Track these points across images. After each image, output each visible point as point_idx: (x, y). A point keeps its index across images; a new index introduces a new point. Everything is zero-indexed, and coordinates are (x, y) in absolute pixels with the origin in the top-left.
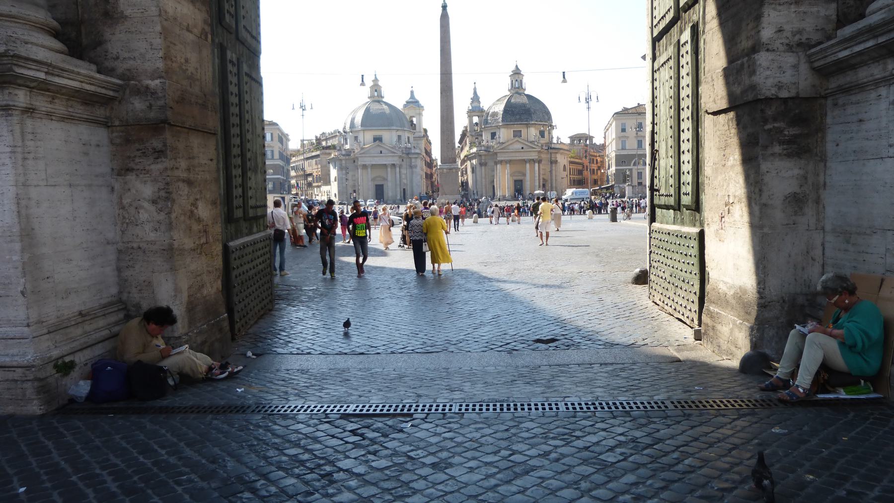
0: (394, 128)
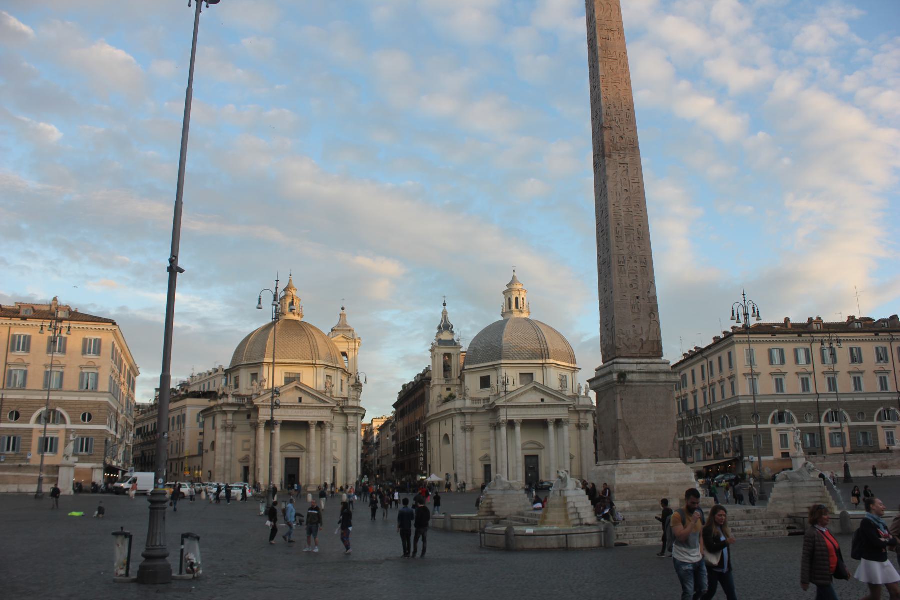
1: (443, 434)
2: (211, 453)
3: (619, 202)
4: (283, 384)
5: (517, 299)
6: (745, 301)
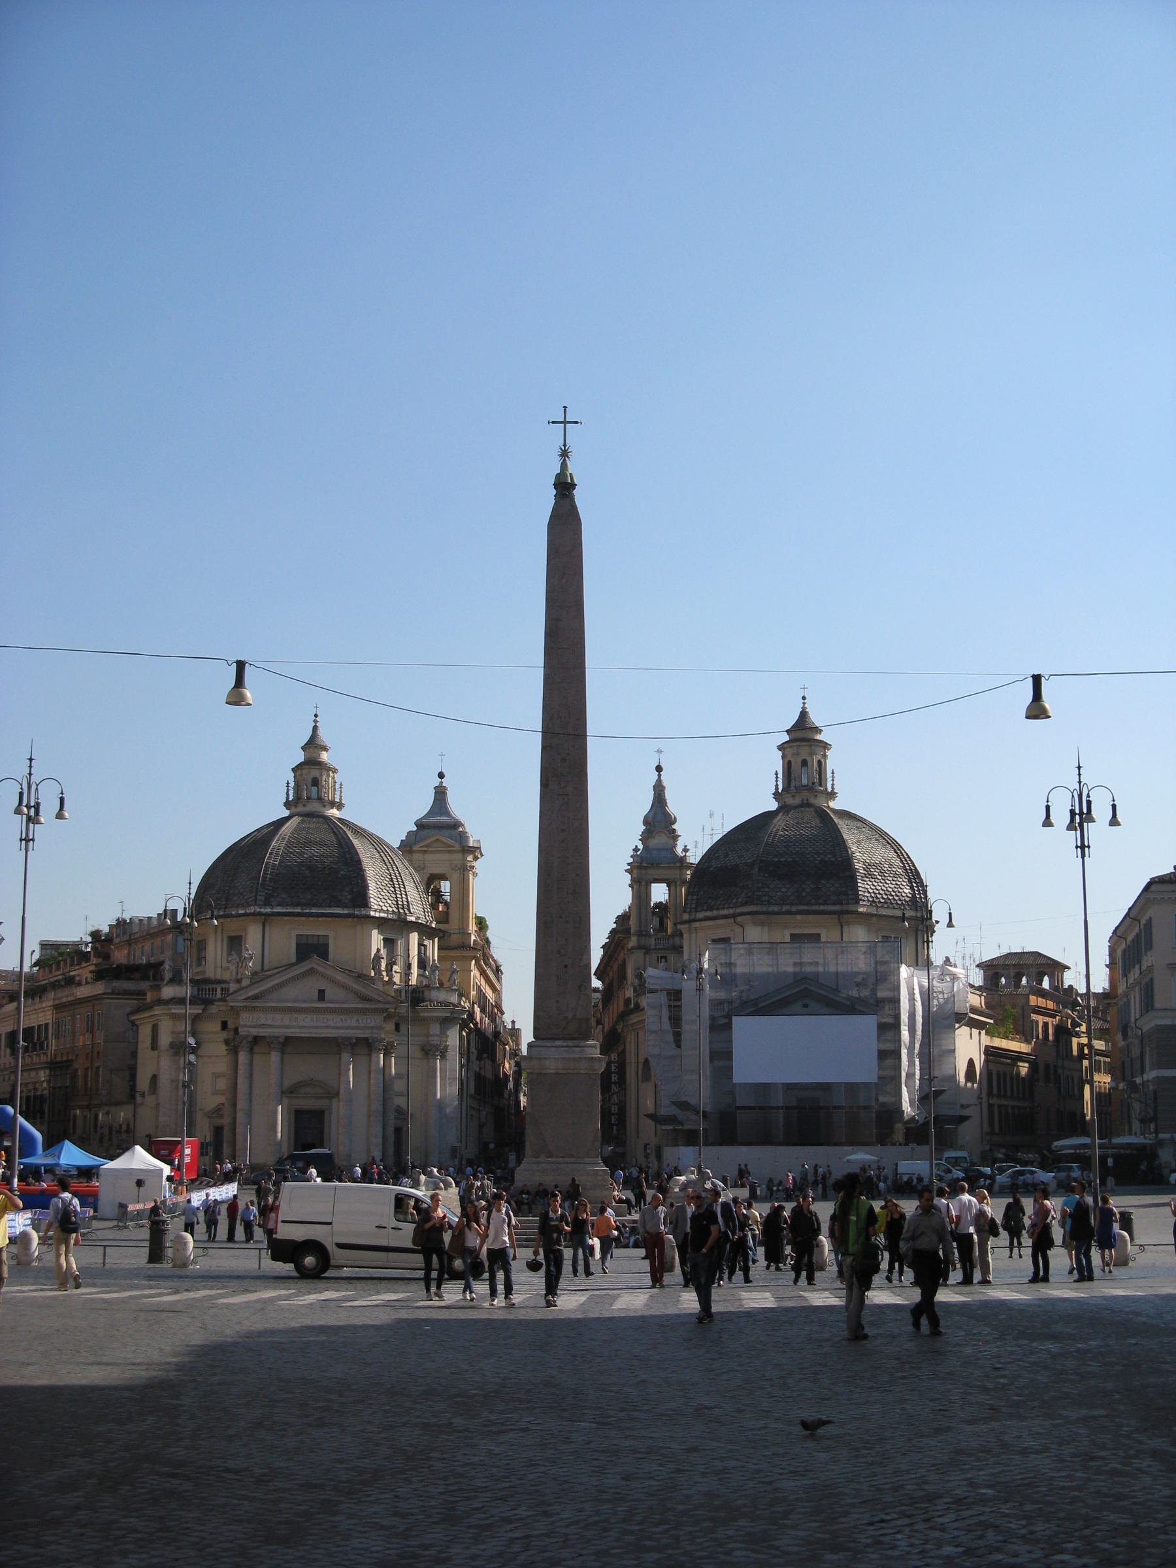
1: (641, 1060)
2: (150, 1100)
4: (293, 959)
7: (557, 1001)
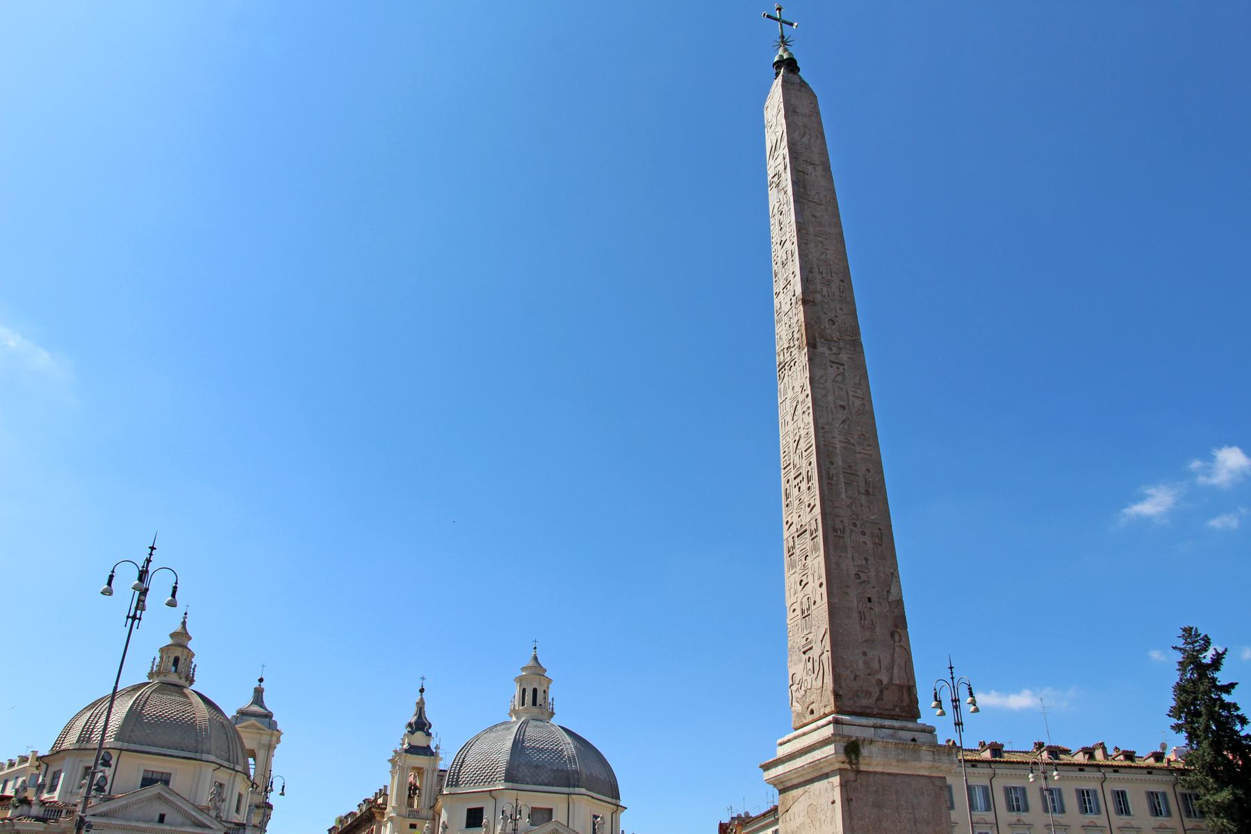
0: (212, 758)
3: (831, 424)
5: (535, 691)
6: (952, 678)
7: (865, 654)
